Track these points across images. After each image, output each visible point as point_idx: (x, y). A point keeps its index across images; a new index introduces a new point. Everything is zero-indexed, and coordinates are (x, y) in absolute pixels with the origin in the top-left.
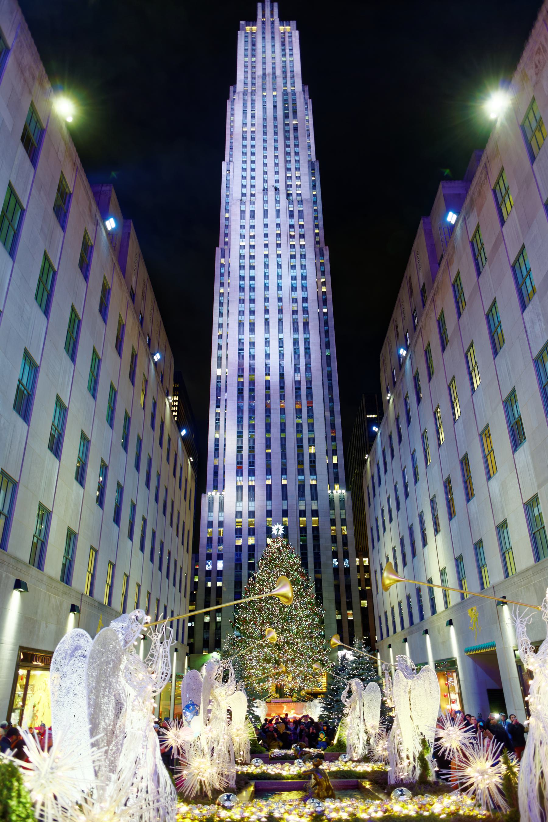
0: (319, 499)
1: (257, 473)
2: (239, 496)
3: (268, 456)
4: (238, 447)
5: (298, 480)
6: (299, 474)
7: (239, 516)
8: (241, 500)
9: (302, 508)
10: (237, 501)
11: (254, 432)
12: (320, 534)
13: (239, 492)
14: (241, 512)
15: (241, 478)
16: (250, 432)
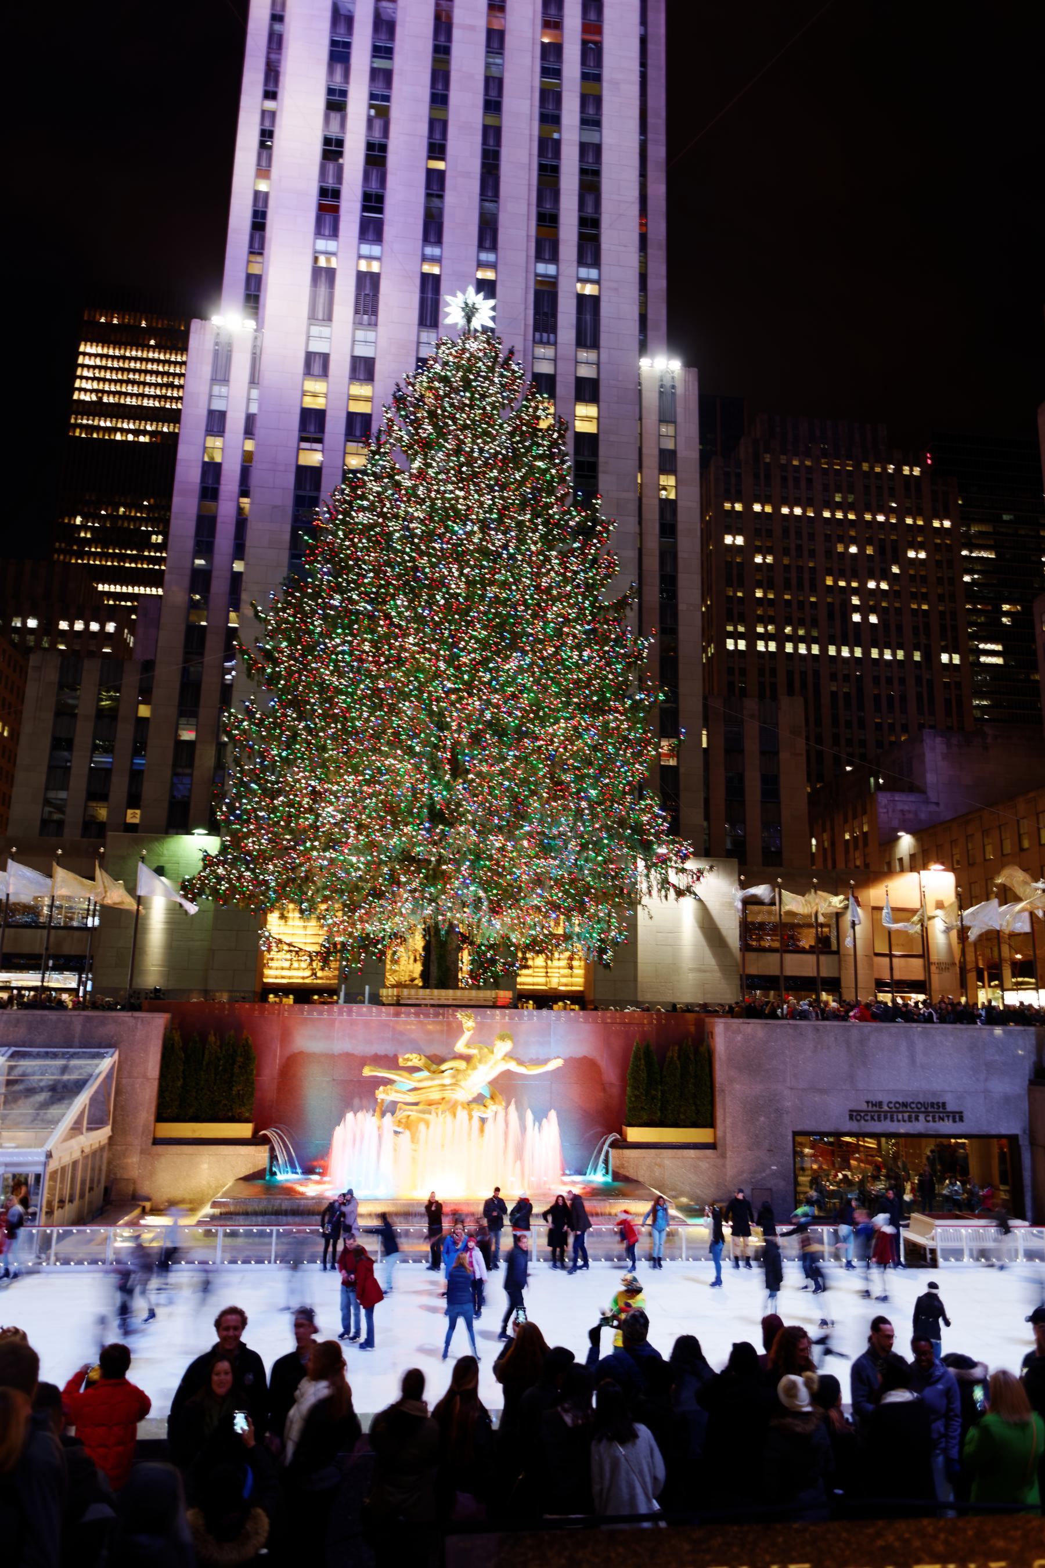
0: (603, 342)
1: (388, 232)
2: (321, 300)
3: (435, 183)
4: (327, 141)
5: (537, 275)
6: (539, 257)
7: (317, 368)
8: (329, 318)
9: (545, 368)
10: (312, 317)
11: (387, 98)
12: (602, 459)
13: (323, 289)
14: (325, 357)
15: (331, 245)
16: (373, 96)
